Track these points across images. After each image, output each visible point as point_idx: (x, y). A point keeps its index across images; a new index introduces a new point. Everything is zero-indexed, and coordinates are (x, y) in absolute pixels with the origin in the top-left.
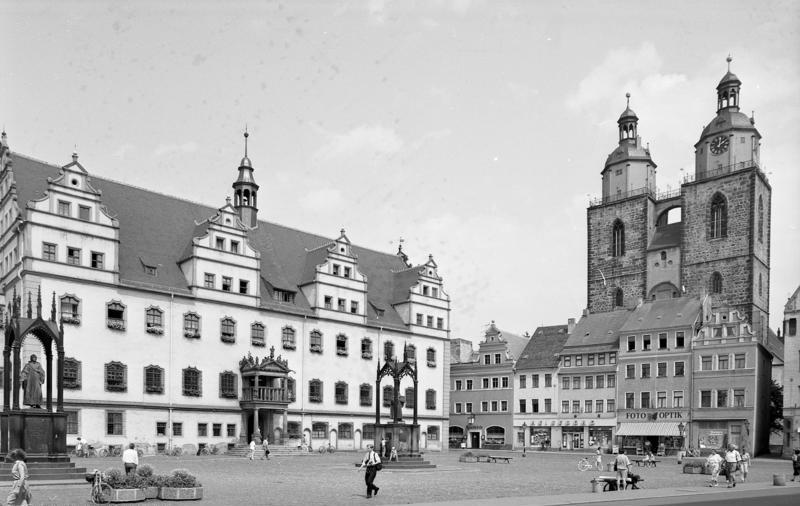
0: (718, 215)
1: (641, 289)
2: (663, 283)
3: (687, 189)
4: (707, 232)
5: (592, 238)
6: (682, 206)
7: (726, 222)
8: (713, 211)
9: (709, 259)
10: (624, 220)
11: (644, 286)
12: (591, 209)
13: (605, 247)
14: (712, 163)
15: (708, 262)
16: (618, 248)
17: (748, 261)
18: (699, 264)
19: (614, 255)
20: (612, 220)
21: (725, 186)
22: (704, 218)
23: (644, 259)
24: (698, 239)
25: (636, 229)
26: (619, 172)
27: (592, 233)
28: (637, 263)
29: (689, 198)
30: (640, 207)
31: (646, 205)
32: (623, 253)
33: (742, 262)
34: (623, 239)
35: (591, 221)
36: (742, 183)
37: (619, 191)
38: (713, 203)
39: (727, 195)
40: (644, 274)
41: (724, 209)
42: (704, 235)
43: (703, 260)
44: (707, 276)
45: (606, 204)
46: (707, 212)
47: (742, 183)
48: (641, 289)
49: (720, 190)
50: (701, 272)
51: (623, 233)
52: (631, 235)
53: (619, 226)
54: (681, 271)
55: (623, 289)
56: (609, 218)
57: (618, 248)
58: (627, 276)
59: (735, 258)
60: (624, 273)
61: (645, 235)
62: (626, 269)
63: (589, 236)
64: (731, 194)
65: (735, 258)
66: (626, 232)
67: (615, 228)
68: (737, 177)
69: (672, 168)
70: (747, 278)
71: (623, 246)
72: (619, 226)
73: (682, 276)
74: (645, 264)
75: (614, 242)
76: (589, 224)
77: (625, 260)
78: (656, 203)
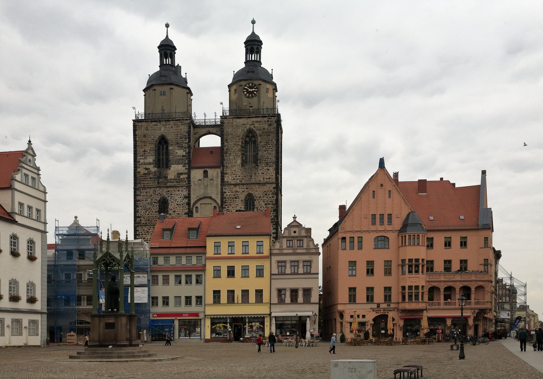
1: (186, 201)
2: (205, 198)
6: (222, 136)
7: (257, 154)
8: (246, 143)
9: (243, 182)
10: (170, 137)
11: (188, 197)
12: (136, 122)
13: (150, 159)
15: (243, 184)
16: (163, 161)
17: (274, 188)
18: (235, 185)
19: (159, 167)
20: (157, 134)
21: (256, 125)
23: (189, 174)
25: (181, 147)
26: (163, 94)
27: (138, 144)
29: (228, 129)
31: (190, 128)
32: (168, 167)
33: (271, 187)
34: (167, 154)
35: (137, 132)
37: (163, 110)
39: (257, 132)
40: (189, 187)
42: (239, 161)
44: (243, 197)
46: (242, 143)
48: (186, 201)
49: (252, 127)
50: (236, 192)
51: (167, 148)
53: (163, 142)
54: (222, 189)
55: (169, 198)
57: (163, 161)
58: (170, 187)
59: (264, 184)
60: (168, 184)
62: (171, 181)
66: (170, 148)
67: (160, 143)
68: (266, 119)
69: (210, 101)
70: (274, 202)
71: (168, 160)
72: (163, 142)
73: (222, 193)
74: (189, 178)
76: (135, 135)
78: (195, 127)
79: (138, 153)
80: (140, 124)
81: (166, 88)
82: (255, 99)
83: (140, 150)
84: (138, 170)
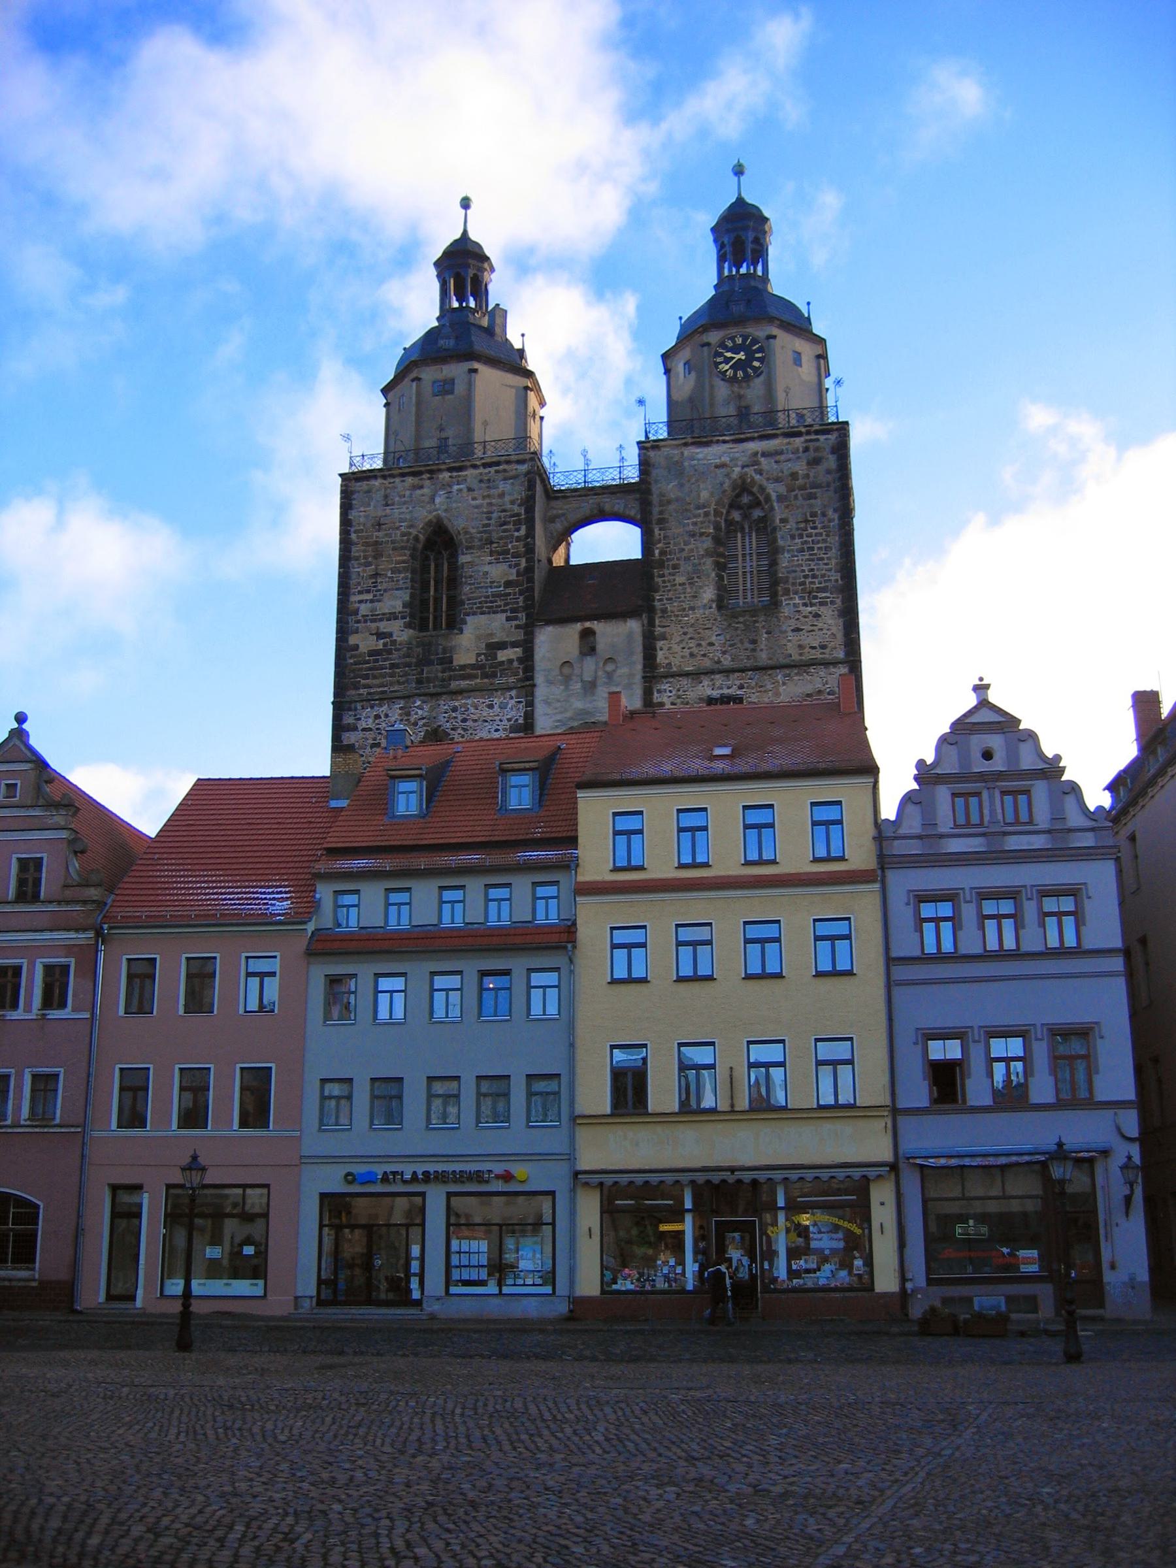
5: (356, 569)
7: (774, 563)
13: (395, 602)
19: (423, 627)
22: (708, 543)
23: (528, 647)
24: (692, 598)
25: (501, 554)
27: (355, 551)
28: (502, 656)
31: (531, 486)
32: (454, 625)
34: (454, 582)
35: (353, 515)
36: (815, 462)
39: (773, 490)
41: (764, 527)
42: (708, 594)
43: (707, 663)
46: (717, 528)
49: (750, 471)
52: (487, 571)
56: (416, 507)
60: (454, 685)
61: (529, 570)
62: (465, 672)
64: (782, 489)
66: (463, 559)
67: (430, 544)
68: (798, 442)
71: (454, 603)
75: (425, 586)
77: (466, 645)
79: (353, 582)
80: (364, 485)
82: (758, 382)
84: (353, 640)
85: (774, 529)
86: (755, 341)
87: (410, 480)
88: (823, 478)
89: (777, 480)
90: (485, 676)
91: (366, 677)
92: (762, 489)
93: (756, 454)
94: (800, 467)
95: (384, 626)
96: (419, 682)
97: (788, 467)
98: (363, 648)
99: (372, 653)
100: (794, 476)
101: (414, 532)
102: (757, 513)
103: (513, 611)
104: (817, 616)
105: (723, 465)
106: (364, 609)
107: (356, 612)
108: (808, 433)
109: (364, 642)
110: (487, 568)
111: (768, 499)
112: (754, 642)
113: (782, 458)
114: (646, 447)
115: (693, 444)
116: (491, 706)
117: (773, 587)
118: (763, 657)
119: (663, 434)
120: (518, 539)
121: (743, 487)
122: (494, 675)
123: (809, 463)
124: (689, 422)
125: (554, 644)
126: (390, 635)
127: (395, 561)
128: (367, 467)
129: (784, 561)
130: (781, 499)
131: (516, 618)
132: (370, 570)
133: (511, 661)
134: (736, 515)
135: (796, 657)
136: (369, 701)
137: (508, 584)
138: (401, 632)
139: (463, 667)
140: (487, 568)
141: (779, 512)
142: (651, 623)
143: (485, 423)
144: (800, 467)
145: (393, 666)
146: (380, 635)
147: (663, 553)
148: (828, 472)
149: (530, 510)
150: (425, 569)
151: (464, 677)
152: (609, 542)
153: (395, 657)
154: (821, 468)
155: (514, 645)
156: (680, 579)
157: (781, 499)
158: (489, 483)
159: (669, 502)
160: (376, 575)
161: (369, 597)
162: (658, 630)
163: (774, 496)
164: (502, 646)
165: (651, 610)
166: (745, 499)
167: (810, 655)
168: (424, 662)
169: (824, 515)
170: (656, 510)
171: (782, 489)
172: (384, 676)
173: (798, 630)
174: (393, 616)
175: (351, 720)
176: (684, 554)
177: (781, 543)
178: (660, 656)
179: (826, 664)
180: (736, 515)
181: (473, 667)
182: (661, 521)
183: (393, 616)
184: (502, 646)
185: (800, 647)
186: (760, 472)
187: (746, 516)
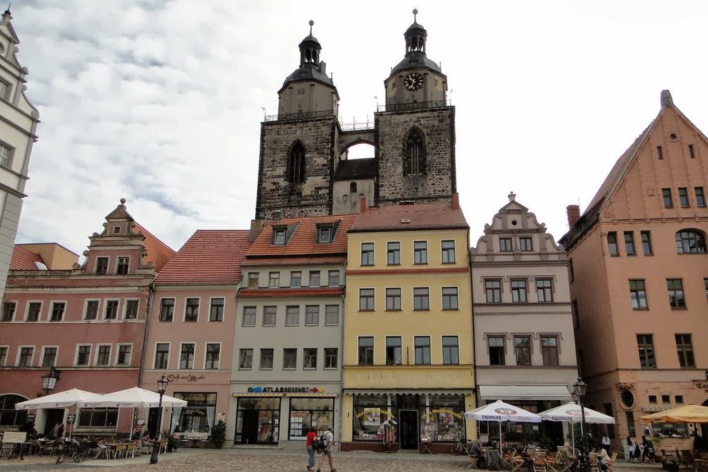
0: (415, 152)
3: (381, 119)
4: (404, 167)
8: (409, 145)
10: (307, 142)
12: (266, 125)
13: (281, 170)
14: (407, 96)
16: (297, 172)
19: (291, 181)
20: (291, 139)
21: (423, 121)
22: (400, 151)
23: (331, 188)
25: (321, 154)
30: (326, 130)
31: (334, 129)
32: (303, 180)
34: (303, 164)
38: (410, 137)
39: (425, 131)
42: (400, 169)
43: (399, 196)
45: (285, 119)
46: (404, 145)
47: (441, 121)
49: (417, 124)
57: (297, 172)
59: (436, 198)
60: (302, 203)
61: (332, 160)
63: (262, 154)
64: (429, 131)
65: (436, 198)
66: (307, 155)
68: (436, 113)
71: (303, 172)
74: (330, 194)
75: (292, 165)
76: (262, 141)
77: (307, 188)
80: (270, 127)
81: (306, 85)
82: (421, 91)
83: (268, 159)
84: (264, 185)
85: (425, 147)
86: (420, 75)
87: (287, 126)
88: (445, 127)
89: (427, 128)
90: (314, 199)
91: (269, 199)
92: (421, 131)
93: (419, 118)
94: (436, 123)
95: (275, 180)
96: (289, 201)
97: (431, 123)
98: (268, 189)
99: (271, 190)
100: (433, 126)
101: (288, 145)
102: (419, 140)
103: (325, 175)
104: (441, 179)
105: (407, 122)
106: (269, 174)
107: (266, 175)
108: (439, 110)
109: (268, 186)
110: (315, 159)
111: (424, 134)
112: (417, 188)
113: (429, 119)
114: (378, 115)
115: (395, 114)
116: (316, 211)
117: (423, 168)
118: (420, 194)
119: (383, 109)
120: (328, 148)
121: (414, 130)
122: (317, 200)
123: (439, 122)
124: (395, 107)
125: (342, 188)
126: (278, 184)
127: (281, 155)
128: (271, 120)
129: (429, 158)
130: (428, 135)
131: (326, 178)
132: (272, 159)
133: (324, 194)
134: (411, 141)
135: (433, 194)
136: (270, 208)
137: (324, 165)
138: (283, 183)
139: (306, 196)
140: (315, 159)
141: (427, 139)
142: (378, 180)
143: (317, 105)
144: (436, 123)
145: (279, 195)
146: (274, 183)
147: (383, 154)
148: (447, 125)
149: (333, 138)
150: (293, 159)
151: (306, 200)
152: (362, 152)
153: (280, 192)
154: (444, 123)
155: (326, 188)
156: (389, 164)
157: (428, 135)
158: (318, 128)
159: (386, 136)
160: (274, 161)
161: (271, 169)
162: (380, 183)
163: (426, 134)
164: (321, 188)
165: (378, 176)
166: (415, 135)
167: (438, 194)
168: (291, 194)
169: (444, 141)
170: (380, 138)
171: (429, 131)
172: (275, 199)
173: (434, 184)
174: (279, 177)
175: (263, 215)
176: (391, 155)
177: (428, 151)
178: (381, 194)
179: (443, 197)
180: (411, 141)
181: (310, 196)
182: (382, 143)
183: (279, 177)
184: (321, 188)
185: (434, 191)
186: (421, 125)
187: (415, 142)
